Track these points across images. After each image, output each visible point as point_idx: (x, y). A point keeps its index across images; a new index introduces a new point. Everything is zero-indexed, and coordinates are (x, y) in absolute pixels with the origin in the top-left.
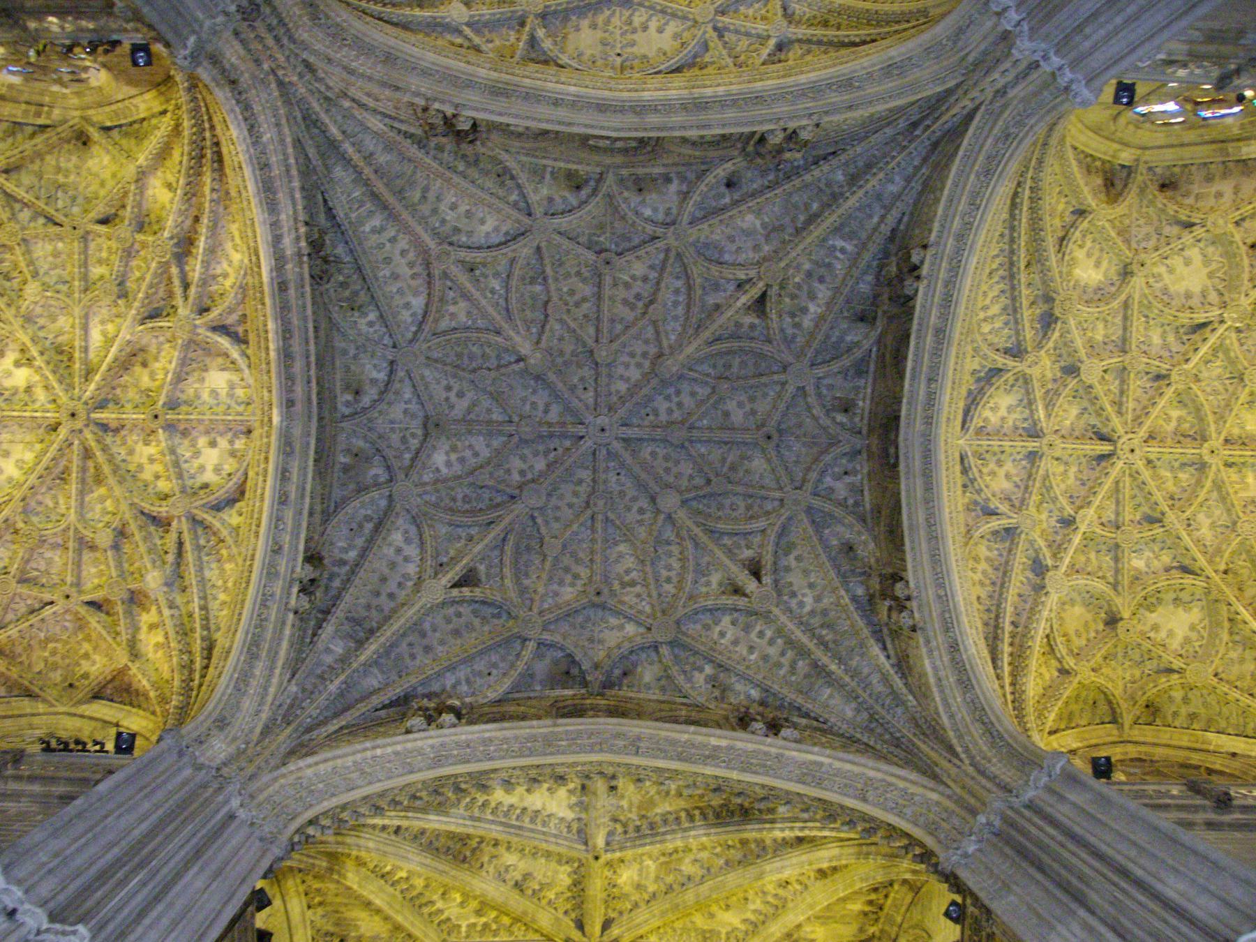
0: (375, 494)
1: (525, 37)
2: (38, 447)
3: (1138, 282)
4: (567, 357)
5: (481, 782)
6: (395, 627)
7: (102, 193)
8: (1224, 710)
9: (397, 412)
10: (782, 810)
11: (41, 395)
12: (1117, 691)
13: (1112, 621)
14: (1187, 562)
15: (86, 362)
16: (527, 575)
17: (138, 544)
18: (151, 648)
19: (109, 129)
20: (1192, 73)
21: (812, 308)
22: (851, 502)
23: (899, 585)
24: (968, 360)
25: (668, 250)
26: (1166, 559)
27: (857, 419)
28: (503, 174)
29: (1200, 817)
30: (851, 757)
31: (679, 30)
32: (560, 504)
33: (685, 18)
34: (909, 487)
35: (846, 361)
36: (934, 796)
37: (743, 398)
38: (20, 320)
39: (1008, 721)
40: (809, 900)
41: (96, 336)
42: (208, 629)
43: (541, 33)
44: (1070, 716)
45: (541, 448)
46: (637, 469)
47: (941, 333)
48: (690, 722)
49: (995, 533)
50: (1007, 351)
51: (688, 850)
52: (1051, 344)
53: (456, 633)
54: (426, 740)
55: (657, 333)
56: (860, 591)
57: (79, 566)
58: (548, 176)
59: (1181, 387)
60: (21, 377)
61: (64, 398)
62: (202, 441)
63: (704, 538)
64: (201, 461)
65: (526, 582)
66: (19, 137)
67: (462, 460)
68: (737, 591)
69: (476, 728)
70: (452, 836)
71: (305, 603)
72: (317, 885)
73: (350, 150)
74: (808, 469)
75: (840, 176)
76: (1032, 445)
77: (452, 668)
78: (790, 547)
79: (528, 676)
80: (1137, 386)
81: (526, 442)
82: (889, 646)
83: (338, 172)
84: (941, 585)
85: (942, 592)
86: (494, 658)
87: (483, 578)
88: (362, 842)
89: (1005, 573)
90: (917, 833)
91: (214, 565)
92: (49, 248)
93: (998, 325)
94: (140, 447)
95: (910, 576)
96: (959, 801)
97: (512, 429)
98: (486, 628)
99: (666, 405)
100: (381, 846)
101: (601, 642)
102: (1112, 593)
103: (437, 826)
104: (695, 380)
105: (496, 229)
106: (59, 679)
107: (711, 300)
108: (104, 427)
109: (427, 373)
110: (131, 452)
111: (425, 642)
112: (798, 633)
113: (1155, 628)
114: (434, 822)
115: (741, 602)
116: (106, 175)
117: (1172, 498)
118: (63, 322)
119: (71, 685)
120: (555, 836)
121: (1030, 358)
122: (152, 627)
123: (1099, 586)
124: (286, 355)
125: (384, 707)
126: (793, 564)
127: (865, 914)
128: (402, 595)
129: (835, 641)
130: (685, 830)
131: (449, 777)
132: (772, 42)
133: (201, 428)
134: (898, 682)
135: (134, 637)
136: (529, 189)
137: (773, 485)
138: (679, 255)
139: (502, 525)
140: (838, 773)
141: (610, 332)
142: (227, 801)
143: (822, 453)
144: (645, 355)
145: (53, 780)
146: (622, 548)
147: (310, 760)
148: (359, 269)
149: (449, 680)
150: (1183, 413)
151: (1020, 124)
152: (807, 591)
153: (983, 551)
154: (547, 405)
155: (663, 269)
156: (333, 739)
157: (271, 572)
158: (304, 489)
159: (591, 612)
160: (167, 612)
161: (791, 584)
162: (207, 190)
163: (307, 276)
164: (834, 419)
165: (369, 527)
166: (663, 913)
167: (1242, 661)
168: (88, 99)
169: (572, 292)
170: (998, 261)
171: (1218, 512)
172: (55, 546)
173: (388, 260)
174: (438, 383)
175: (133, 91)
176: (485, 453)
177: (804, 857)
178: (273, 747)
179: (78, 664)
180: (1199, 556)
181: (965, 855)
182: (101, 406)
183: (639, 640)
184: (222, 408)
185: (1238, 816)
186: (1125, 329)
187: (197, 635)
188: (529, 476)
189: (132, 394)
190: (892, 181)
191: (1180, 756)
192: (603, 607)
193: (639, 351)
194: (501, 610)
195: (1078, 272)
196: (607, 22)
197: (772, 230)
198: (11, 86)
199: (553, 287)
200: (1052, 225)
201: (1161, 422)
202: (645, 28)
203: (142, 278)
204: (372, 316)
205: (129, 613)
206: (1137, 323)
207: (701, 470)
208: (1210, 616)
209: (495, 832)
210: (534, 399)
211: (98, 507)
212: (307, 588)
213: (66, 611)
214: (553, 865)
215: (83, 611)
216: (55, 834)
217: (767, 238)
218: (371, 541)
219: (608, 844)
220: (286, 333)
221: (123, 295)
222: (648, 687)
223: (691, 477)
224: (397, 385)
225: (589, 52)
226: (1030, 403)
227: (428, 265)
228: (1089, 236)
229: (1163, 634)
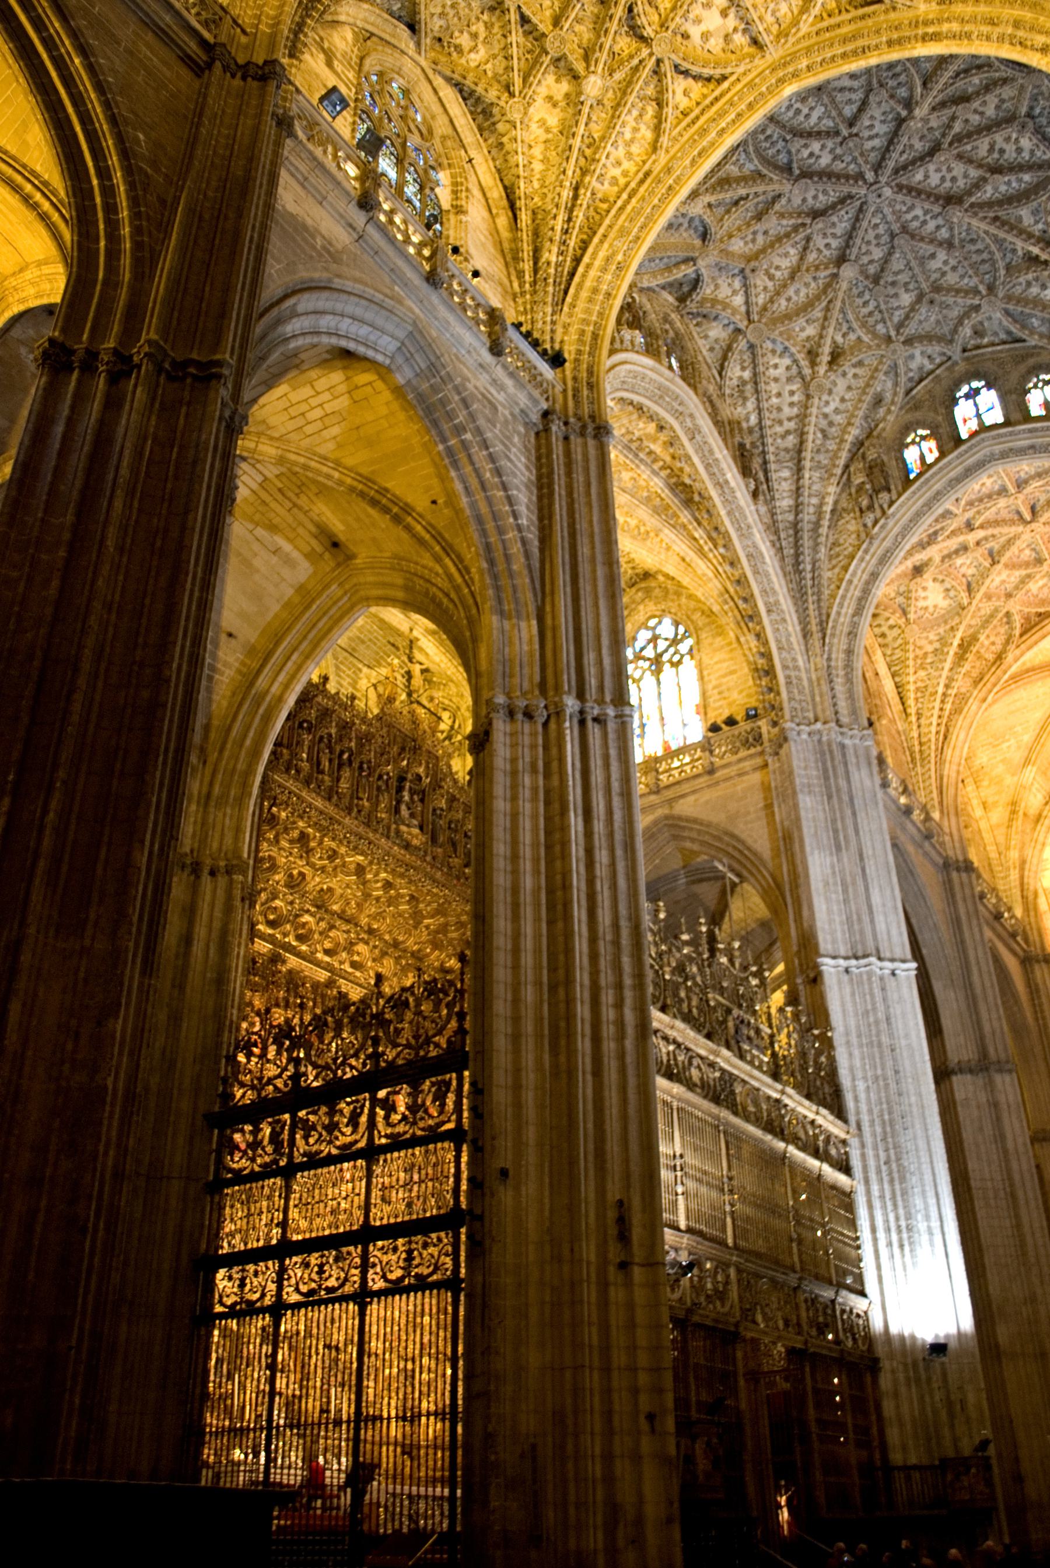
22: (911, 374)
35: (1015, 329)
64: (705, 14)
67: (798, 112)
68: (812, 355)
76: (1012, 489)
101: (717, 286)
113: (924, 589)
115: (807, 371)
119: (440, 40)
126: (850, 375)
137: (896, 319)
140: (767, 575)
144: (954, 179)
167: (931, 642)
179: (462, 32)
193: (955, 173)
208: (948, 612)
222: (706, 337)
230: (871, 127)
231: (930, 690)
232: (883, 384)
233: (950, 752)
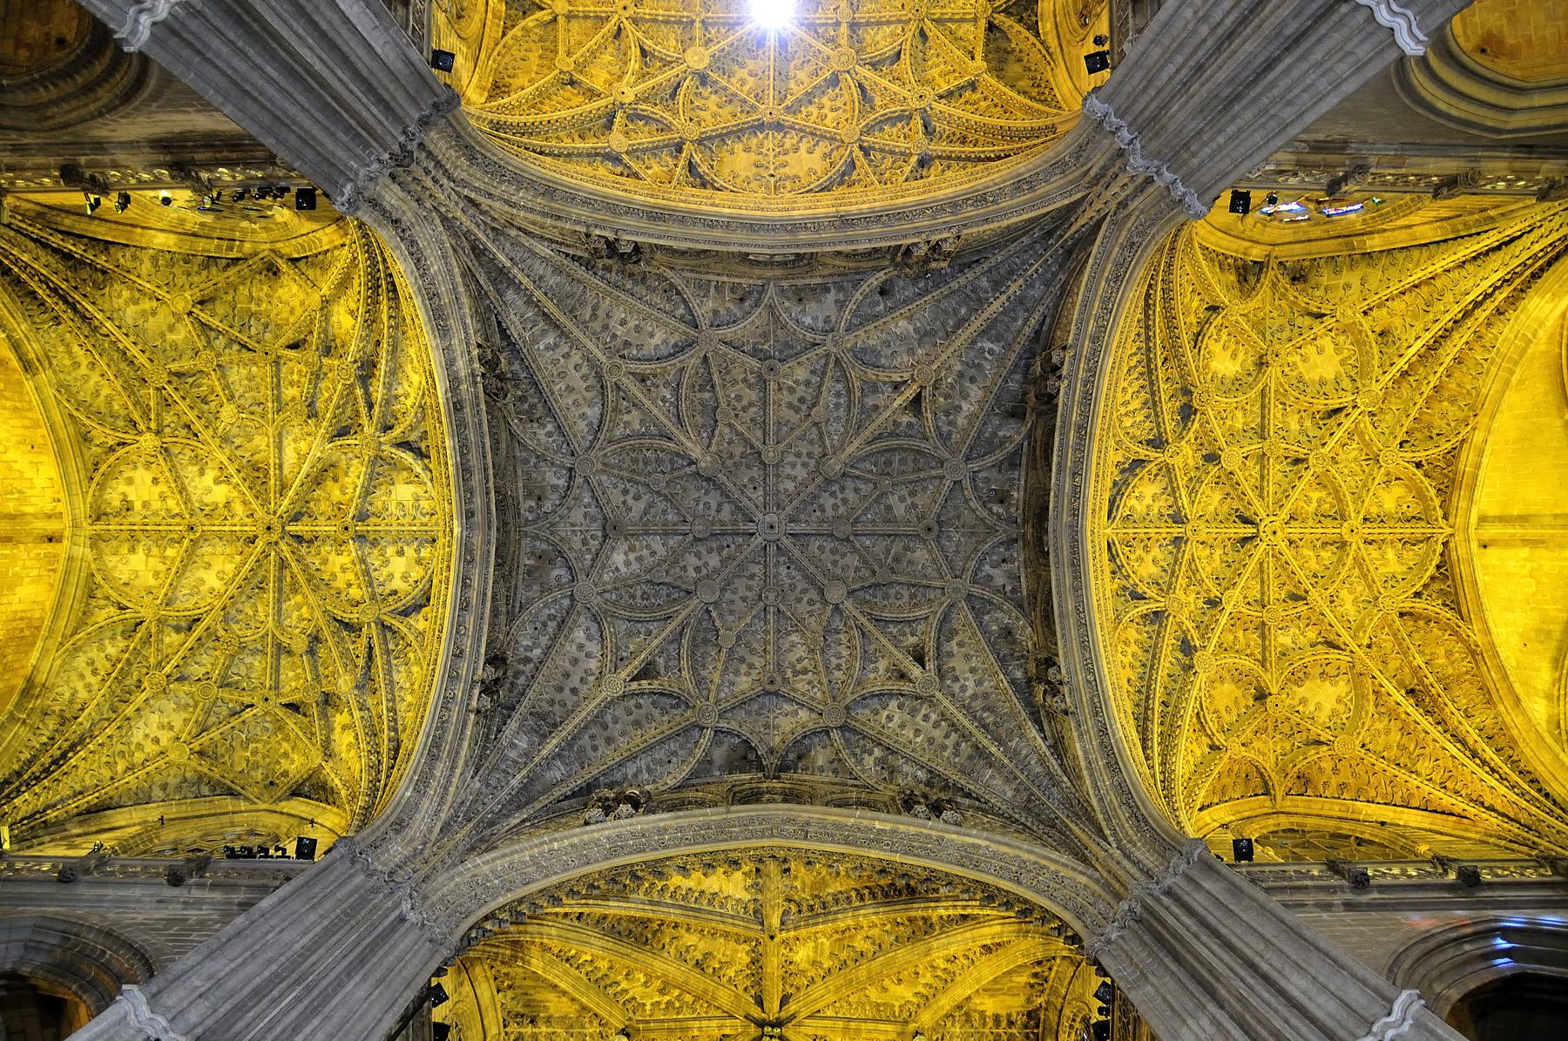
0: (558, 594)
1: (681, 163)
2: (238, 558)
3: (1273, 371)
4: (737, 458)
5: (657, 869)
6: (576, 721)
7: (292, 320)
8: (1372, 779)
9: (577, 516)
10: (943, 891)
11: (239, 509)
12: (1268, 764)
13: (1261, 696)
14: (1332, 637)
15: (281, 478)
16: (704, 666)
17: (329, 651)
18: (344, 748)
19: (298, 260)
20: (1303, 181)
21: (965, 406)
22: (1009, 588)
23: (1051, 671)
24: (1111, 452)
25: (828, 355)
26: (1312, 634)
27: (1013, 510)
28: (671, 290)
29: (1338, 899)
30: (1006, 840)
31: (827, 151)
32: (733, 597)
33: (833, 139)
34: (1059, 577)
35: (999, 455)
36: (1083, 880)
37: (905, 492)
38: (218, 440)
39: (1154, 801)
40: (976, 974)
41: (290, 456)
42: (396, 731)
43: (697, 159)
44: (1224, 789)
45: (714, 545)
46: (805, 563)
47: (1084, 430)
48: (860, 804)
49: (1144, 616)
50: (1149, 442)
51: (858, 927)
52: (1191, 435)
53: (637, 724)
54: (605, 831)
55: (821, 434)
56: (1019, 674)
57: (278, 671)
58: (712, 290)
59: (1319, 470)
60: (220, 493)
61: (260, 513)
62: (390, 551)
63: (869, 627)
64: (390, 568)
65: (703, 673)
66: (214, 270)
67: (640, 559)
69: (652, 817)
70: (632, 920)
71: (487, 702)
72: (504, 970)
73: (520, 276)
74: (968, 559)
75: (984, 282)
76: (1176, 531)
77: (633, 758)
78: (953, 632)
79: (706, 763)
80: (1276, 470)
81: (700, 540)
82: (1046, 727)
83: (510, 295)
84: (1090, 671)
85: (1090, 678)
86: (673, 746)
87: (662, 671)
88: (545, 930)
89: (1154, 656)
90: (1067, 916)
91: (402, 669)
92: (244, 372)
93: (1140, 418)
94: (333, 557)
95: (1061, 661)
96: (1107, 886)
97: (686, 528)
98: (666, 718)
99: (832, 501)
100: (563, 933)
102: (1260, 669)
103: (617, 912)
104: (858, 477)
105: (665, 341)
106: (260, 777)
107: (870, 401)
108: (299, 539)
109: (604, 478)
110: (325, 562)
111: (606, 734)
112: (961, 717)
113: (1303, 701)
114: (614, 908)
115: (906, 687)
116: (295, 303)
117: (1315, 576)
118: (260, 441)
120: (732, 917)
121: (1172, 449)
122: (344, 728)
123: (1248, 663)
124: (464, 470)
125: (567, 798)
127: (1032, 986)
128: (583, 691)
129: (995, 724)
130: (856, 909)
131: (625, 866)
132: (914, 159)
133: (389, 538)
134: (1053, 762)
135: (328, 737)
136: (694, 304)
137: (935, 574)
138: (837, 361)
139: (678, 620)
140: (995, 855)
141: (777, 434)
142: (398, 905)
143: (979, 543)
144: (809, 455)
145: (235, 887)
146: (795, 638)
147: (487, 857)
148: (535, 384)
149: (631, 769)
150: (1324, 494)
151: (1143, 234)
152: (968, 675)
153: (1132, 634)
154: (720, 505)
155: (824, 373)
156: (515, 831)
157: (452, 676)
158: (485, 594)
159: (766, 699)
160: (357, 714)
161: (954, 669)
162: (385, 317)
163: (482, 394)
164: (990, 510)
165: (552, 625)
166: (838, 989)
167: (1388, 732)
168: (276, 234)
169: (739, 398)
170: (1135, 359)
171: (1360, 588)
172: (255, 652)
173: (562, 375)
174: (615, 487)
175: (315, 226)
176: (662, 552)
177: (968, 934)
178: (450, 845)
180: (1342, 631)
181: (1109, 942)
182: (296, 518)
183: (811, 725)
184: (408, 519)
185: (1375, 895)
186: (1263, 417)
187: (385, 737)
188: (704, 572)
189: (324, 507)
190: (1032, 286)
191: (1331, 825)
192: (777, 694)
194: (679, 701)
195: (1215, 365)
197: (925, 335)
198: (202, 224)
199: (720, 395)
200: (1187, 322)
201: (1302, 504)
202: (796, 150)
203: (330, 399)
204: (550, 427)
205: (324, 715)
206: (1275, 412)
207: (866, 562)
209: (674, 915)
210: (706, 499)
211: (296, 614)
212: (489, 689)
213: (267, 713)
214: (732, 943)
215: (281, 713)
216: (210, 956)
217: (921, 343)
218: (554, 639)
219: (783, 923)
220: (463, 449)
221: (312, 413)
222: (821, 769)
223: (857, 569)
224: (576, 491)
225: (743, 174)
226: (1174, 492)
227: (599, 377)
228: (1224, 332)
229: (1311, 708)
230: (707, 506)
231: (1450, 765)
232: (999, 618)
233: (1555, 786)
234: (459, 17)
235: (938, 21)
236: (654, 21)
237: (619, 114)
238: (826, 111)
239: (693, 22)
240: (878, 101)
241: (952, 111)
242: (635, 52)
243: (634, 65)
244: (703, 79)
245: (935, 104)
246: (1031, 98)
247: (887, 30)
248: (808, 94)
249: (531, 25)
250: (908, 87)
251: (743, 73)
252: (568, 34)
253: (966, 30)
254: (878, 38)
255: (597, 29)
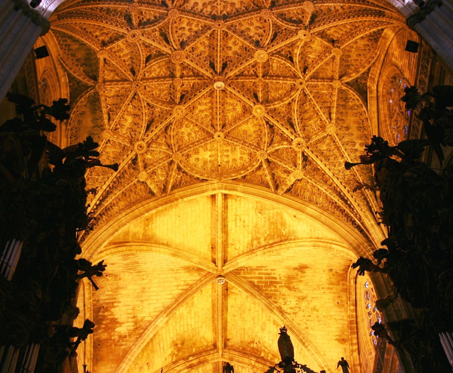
196: (225, 7)
202: (204, 5)
234: (394, 78)
235: (126, 80)
236: (285, 77)
237: (307, 23)
238: (187, 28)
239: (263, 77)
240: (157, 33)
241: (116, 29)
242: (296, 59)
243: (297, 51)
244: (257, 44)
245: (126, 32)
246: (71, 37)
247: (153, 75)
248: (198, 37)
249: (354, 74)
250: (141, 42)
251: (235, 48)
252: (335, 69)
253: (109, 76)
254: (158, 70)
255: (317, 72)
